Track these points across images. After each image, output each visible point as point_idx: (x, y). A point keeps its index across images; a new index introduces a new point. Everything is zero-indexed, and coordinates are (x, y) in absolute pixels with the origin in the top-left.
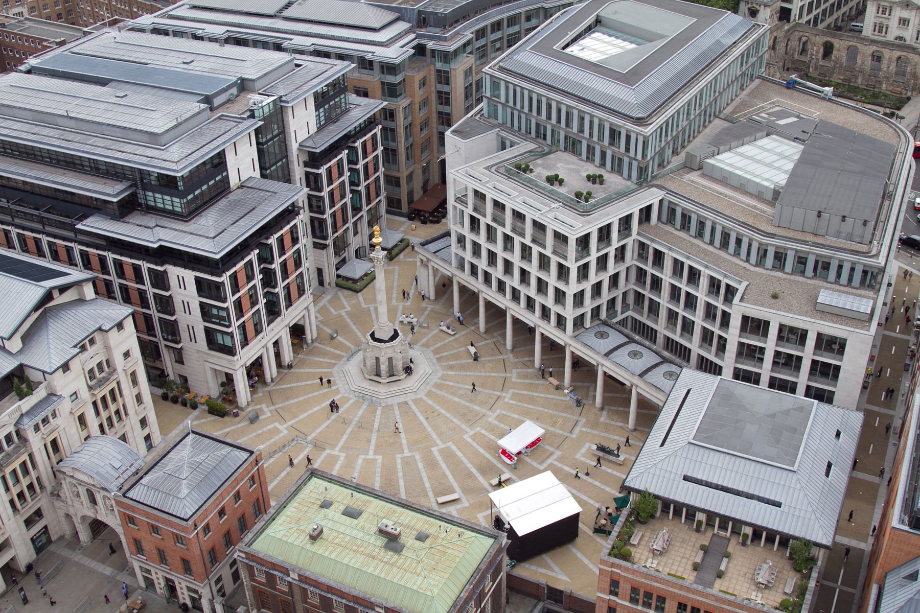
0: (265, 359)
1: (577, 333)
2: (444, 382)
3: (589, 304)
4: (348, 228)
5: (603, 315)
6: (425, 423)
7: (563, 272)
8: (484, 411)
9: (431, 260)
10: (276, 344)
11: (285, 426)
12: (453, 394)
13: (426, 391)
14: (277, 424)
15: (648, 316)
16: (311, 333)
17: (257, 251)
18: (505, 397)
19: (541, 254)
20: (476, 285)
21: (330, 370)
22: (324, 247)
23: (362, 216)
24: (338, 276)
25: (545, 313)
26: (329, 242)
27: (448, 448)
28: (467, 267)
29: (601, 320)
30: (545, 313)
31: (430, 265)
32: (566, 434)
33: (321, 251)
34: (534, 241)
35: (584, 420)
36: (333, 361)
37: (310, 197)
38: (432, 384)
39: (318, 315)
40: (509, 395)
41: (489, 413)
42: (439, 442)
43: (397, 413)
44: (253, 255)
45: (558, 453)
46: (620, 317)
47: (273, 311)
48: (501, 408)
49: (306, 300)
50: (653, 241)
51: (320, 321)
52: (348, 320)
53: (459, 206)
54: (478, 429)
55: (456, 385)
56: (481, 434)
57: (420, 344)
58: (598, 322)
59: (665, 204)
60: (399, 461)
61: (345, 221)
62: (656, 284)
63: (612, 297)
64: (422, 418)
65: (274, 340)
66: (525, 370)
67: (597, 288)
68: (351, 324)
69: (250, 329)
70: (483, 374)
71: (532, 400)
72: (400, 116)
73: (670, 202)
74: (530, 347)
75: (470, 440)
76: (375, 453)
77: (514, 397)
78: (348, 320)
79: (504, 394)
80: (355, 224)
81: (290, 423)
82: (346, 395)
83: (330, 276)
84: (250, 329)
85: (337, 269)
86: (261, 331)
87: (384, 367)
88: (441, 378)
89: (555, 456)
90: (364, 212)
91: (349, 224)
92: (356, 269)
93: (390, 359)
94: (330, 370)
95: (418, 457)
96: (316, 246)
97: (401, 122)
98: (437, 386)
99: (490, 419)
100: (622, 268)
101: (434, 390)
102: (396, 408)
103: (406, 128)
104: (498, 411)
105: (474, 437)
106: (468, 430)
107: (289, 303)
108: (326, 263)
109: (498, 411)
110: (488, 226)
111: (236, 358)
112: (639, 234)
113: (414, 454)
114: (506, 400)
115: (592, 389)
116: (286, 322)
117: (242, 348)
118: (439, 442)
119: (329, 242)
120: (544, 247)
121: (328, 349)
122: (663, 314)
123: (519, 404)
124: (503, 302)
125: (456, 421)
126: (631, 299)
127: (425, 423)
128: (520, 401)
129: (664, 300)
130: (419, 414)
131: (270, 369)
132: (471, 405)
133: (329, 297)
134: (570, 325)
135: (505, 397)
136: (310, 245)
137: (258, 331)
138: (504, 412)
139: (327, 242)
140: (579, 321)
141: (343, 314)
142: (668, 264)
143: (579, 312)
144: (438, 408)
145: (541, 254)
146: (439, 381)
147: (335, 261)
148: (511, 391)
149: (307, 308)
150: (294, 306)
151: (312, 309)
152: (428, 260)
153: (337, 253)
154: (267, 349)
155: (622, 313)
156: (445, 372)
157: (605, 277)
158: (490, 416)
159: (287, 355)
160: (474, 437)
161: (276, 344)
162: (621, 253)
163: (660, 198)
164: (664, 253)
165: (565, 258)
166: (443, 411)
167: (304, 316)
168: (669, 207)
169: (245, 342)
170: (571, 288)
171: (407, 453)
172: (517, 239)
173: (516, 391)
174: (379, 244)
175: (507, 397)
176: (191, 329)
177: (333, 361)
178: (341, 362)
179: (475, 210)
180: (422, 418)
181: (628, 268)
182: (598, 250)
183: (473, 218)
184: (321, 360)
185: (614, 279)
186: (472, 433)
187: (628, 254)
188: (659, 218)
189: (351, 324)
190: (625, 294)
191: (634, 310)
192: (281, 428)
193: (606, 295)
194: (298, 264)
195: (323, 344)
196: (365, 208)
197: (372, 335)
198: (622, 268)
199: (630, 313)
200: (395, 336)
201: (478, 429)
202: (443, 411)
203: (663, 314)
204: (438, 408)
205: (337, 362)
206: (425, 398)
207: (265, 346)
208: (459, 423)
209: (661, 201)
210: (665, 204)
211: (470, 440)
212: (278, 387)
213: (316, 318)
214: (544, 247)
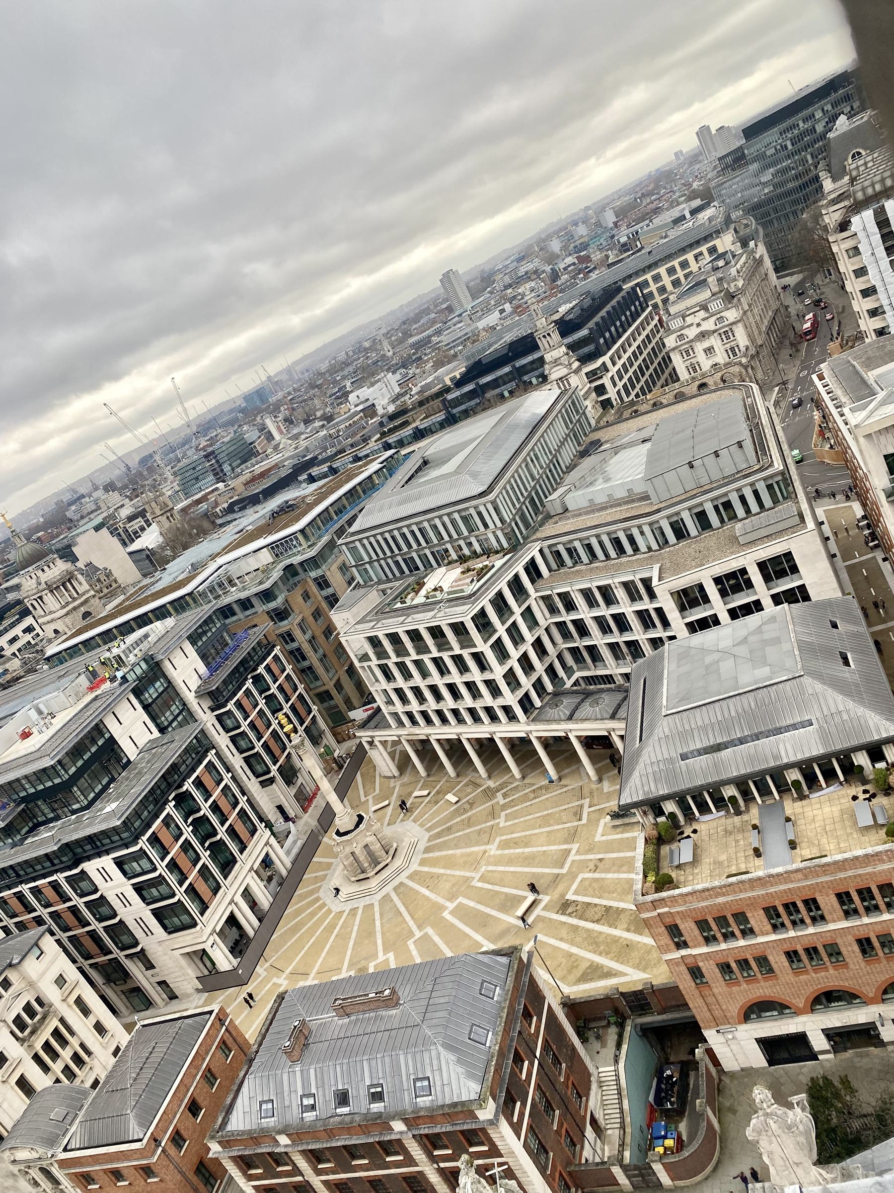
5: (549, 687)
8: (483, 848)
9: (374, 737)
13: (418, 861)
20: (422, 731)
28: (405, 719)
29: (550, 694)
31: (376, 740)
45: (575, 847)
46: (569, 684)
58: (548, 697)
59: (547, 551)
63: (547, 665)
72: (297, 633)
73: (550, 547)
74: (504, 766)
76: (386, 950)
79: (497, 821)
88: (429, 841)
89: (573, 852)
97: (301, 639)
98: (427, 850)
99: (492, 853)
100: (541, 632)
103: (310, 641)
111: (198, 927)
112: (536, 591)
114: (501, 825)
122: (606, 653)
124: (451, 731)
129: (598, 639)
134: (518, 711)
140: (526, 703)
142: (579, 600)
149: (267, 843)
152: (372, 737)
163: (538, 548)
175: (502, 822)
176: (140, 921)
185: (538, 645)
188: (550, 570)
190: (560, 657)
198: (541, 632)
199: (578, 675)
203: (606, 653)
206: (420, 868)
210: (547, 551)
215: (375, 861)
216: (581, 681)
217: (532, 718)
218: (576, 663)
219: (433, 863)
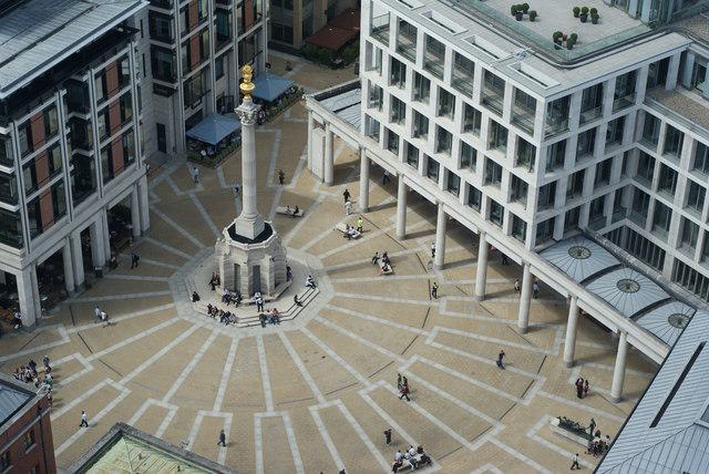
0: (67, 255)
1: (540, 247)
2: (335, 308)
3: (561, 207)
4: (208, 67)
5: (584, 222)
6: (302, 368)
7: (525, 152)
10: (86, 234)
11: (91, 358)
12: (350, 328)
14: (78, 356)
15: (653, 229)
16: (140, 221)
17: (65, 92)
18: (426, 337)
19: (494, 123)
21: (164, 279)
22: (171, 92)
23: (231, 50)
24: (188, 138)
25: (495, 212)
26: (179, 85)
27: (335, 409)
30: (495, 212)
31: (330, 128)
32: (515, 399)
33: (164, 99)
34: (485, 102)
35: (544, 379)
36: (172, 267)
37: (152, 15)
38: (316, 311)
39: (155, 196)
40: (433, 335)
41: (400, 359)
42: (321, 398)
43: (261, 350)
44: (59, 97)
45: (500, 428)
46: (609, 228)
47: (84, 187)
48: (418, 354)
49: (137, 170)
50: (666, 114)
51: (155, 205)
52: (199, 206)
53: (376, 44)
54: (382, 382)
55: (354, 313)
56: (386, 390)
57: (305, 248)
60: (258, 423)
61: (203, 56)
62: (668, 178)
64: (298, 361)
65: (83, 228)
66: (460, 298)
67: (578, 180)
68: (202, 211)
69: (47, 208)
70: (396, 300)
71: (466, 344)
73: (698, 57)
75: (368, 399)
77: (440, 338)
78: (199, 206)
79: (425, 333)
80: (219, 60)
81: (97, 355)
82: (186, 318)
83: (177, 134)
84: (47, 208)
85: (188, 128)
86: (64, 214)
87: (245, 281)
88: (332, 302)
89: (495, 432)
90: (234, 45)
91: (211, 61)
92: (217, 130)
93: (256, 270)
94: (164, 279)
95: (287, 419)
96: (157, 90)
98: (325, 313)
100: (617, 153)
101: (320, 319)
102: (260, 342)
104: (414, 358)
105: (373, 395)
106: (367, 383)
107: (110, 173)
108: (171, 117)
109: (414, 358)
110: (418, 76)
112: (646, 102)
113: (283, 413)
114: (428, 342)
115: (559, 333)
116: (103, 202)
117: (32, 238)
118: (321, 398)
119: (179, 85)
120: (500, 113)
121: (165, 246)
122: (675, 225)
123: (448, 349)
125: (349, 368)
126: (628, 201)
127: (302, 368)
128: (448, 345)
130: (293, 353)
131: (74, 272)
132: (374, 346)
133: (172, 169)
134: (530, 233)
135: (426, 337)
136: (147, 90)
137: (58, 215)
138: (423, 360)
139: (175, 86)
141: (192, 196)
143: (546, 215)
144: (323, 346)
145: (494, 123)
146: (328, 306)
147: (185, 114)
148: (437, 328)
149: (136, 183)
150: (117, 179)
151: (144, 183)
153: (188, 103)
154: (71, 241)
155: (614, 221)
156: (339, 294)
157: (590, 165)
158: (402, 364)
159: (102, 251)
160: (373, 395)
161: (86, 234)
162: (616, 132)
163: (683, 49)
164: (683, 134)
165: (531, 133)
166: (331, 353)
167: (131, 195)
168: (695, 64)
169: (39, 229)
170: (533, 178)
171: (271, 412)
172: (460, 99)
173: (443, 329)
174: (250, 93)
177: (172, 267)
178: (181, 269)
179: (400, 49)
180: (298, 361)
181: (626, 154)
182: (582, 122)
183: (394, 62)
184: (154, 262)
185: (604, 170)
186: (372, 388)
187: (628, 132)
188: (680, 80)
189: (202, 211)
190: (619, 193)
191: (632, 218)
192: (84, 361)
193: (589, 194)
194: (124, 120)
195: (158, 240)
196: (236, 39)
197: (232, 232)
198: (617, 153)
199: (627, 222)
200: (267, 232)
201: (382, 382)
202: (331, 353)
203: (675, 225)
204: (323, 346)
205: (177, 267)
206: (305, 331)
207: (69, 237)
208: (354, 372)
209: (684, 55)
210: (691, 59)
211: (368, 399)
212: (84, 300)
213: (150, 198)
214: (500, 113)
215: (257, 286)
216: (624, 233)
217: (540, 247)
218: (634, 207)
219: (325, 334)
